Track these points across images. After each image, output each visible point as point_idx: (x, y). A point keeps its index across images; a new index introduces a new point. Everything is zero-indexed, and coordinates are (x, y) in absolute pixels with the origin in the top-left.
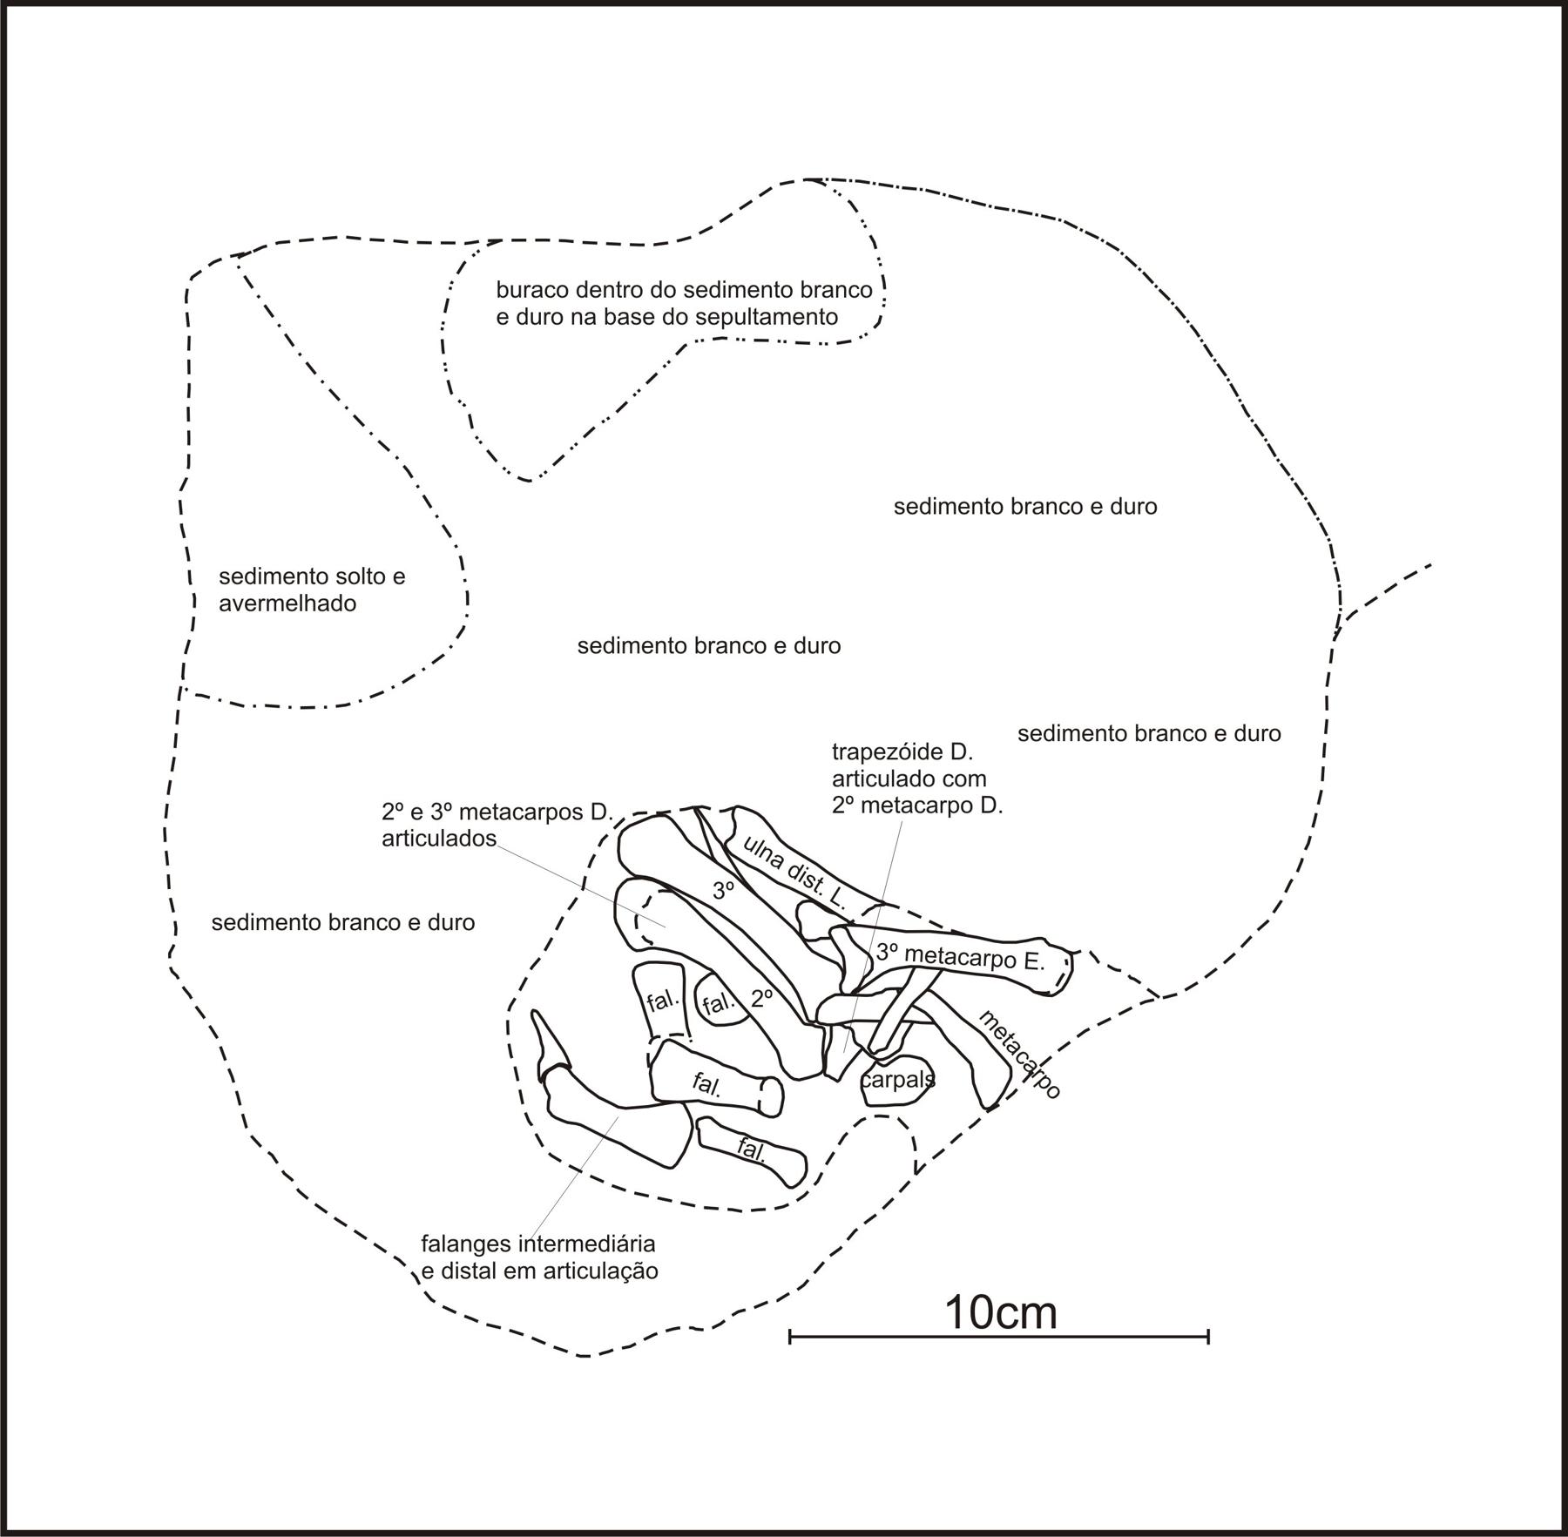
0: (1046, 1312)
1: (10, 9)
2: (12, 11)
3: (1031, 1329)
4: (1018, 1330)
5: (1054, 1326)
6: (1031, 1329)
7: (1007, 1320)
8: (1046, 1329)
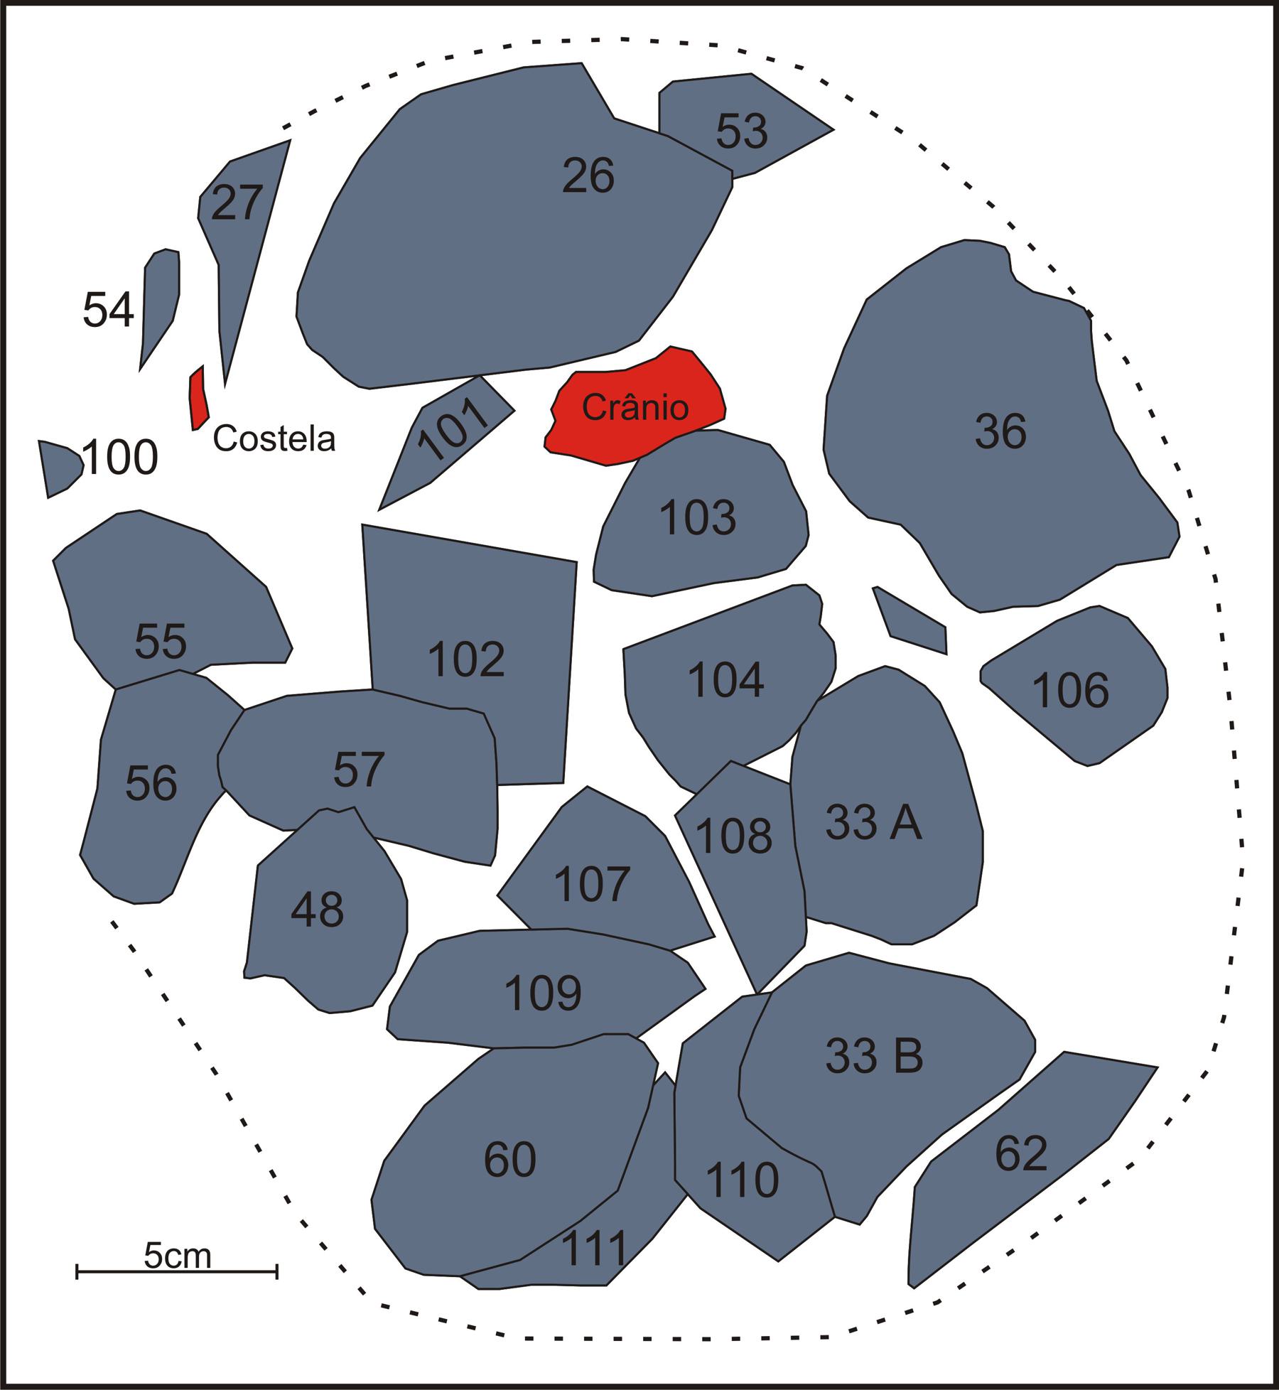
0: (203, 1256)
1: (8, 8)
2: (8, 8)
7: (173, 1263)
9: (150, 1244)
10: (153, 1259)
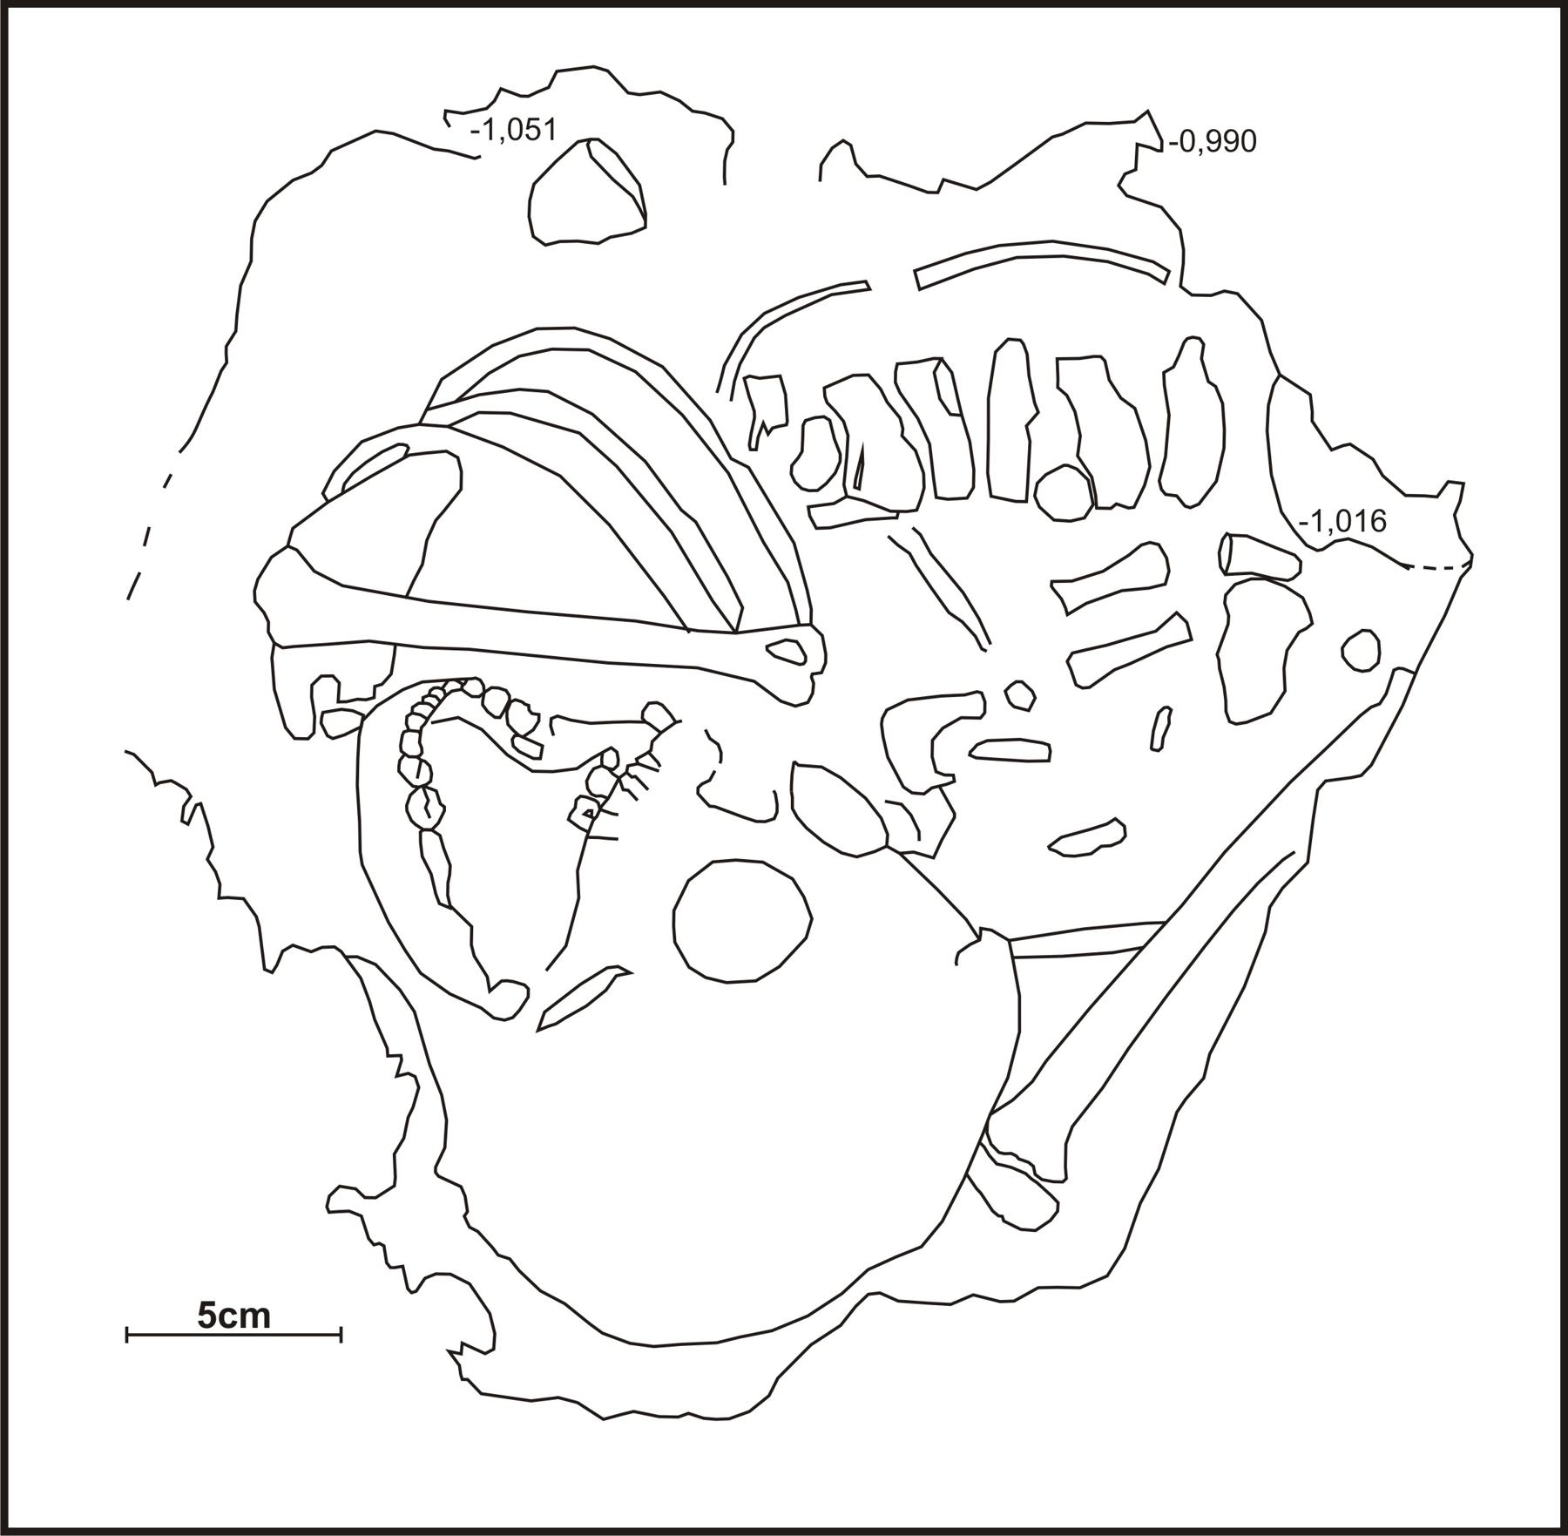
0: (261, 1316)
1: (12, 11)
2: (12, 11)
3: (249, 1329)
4: (237, 1329)
5: (267, 1325)
6: (249, 1329)
8: (261, 1329)
9: (204, 1304)
10: (207, 1319)
